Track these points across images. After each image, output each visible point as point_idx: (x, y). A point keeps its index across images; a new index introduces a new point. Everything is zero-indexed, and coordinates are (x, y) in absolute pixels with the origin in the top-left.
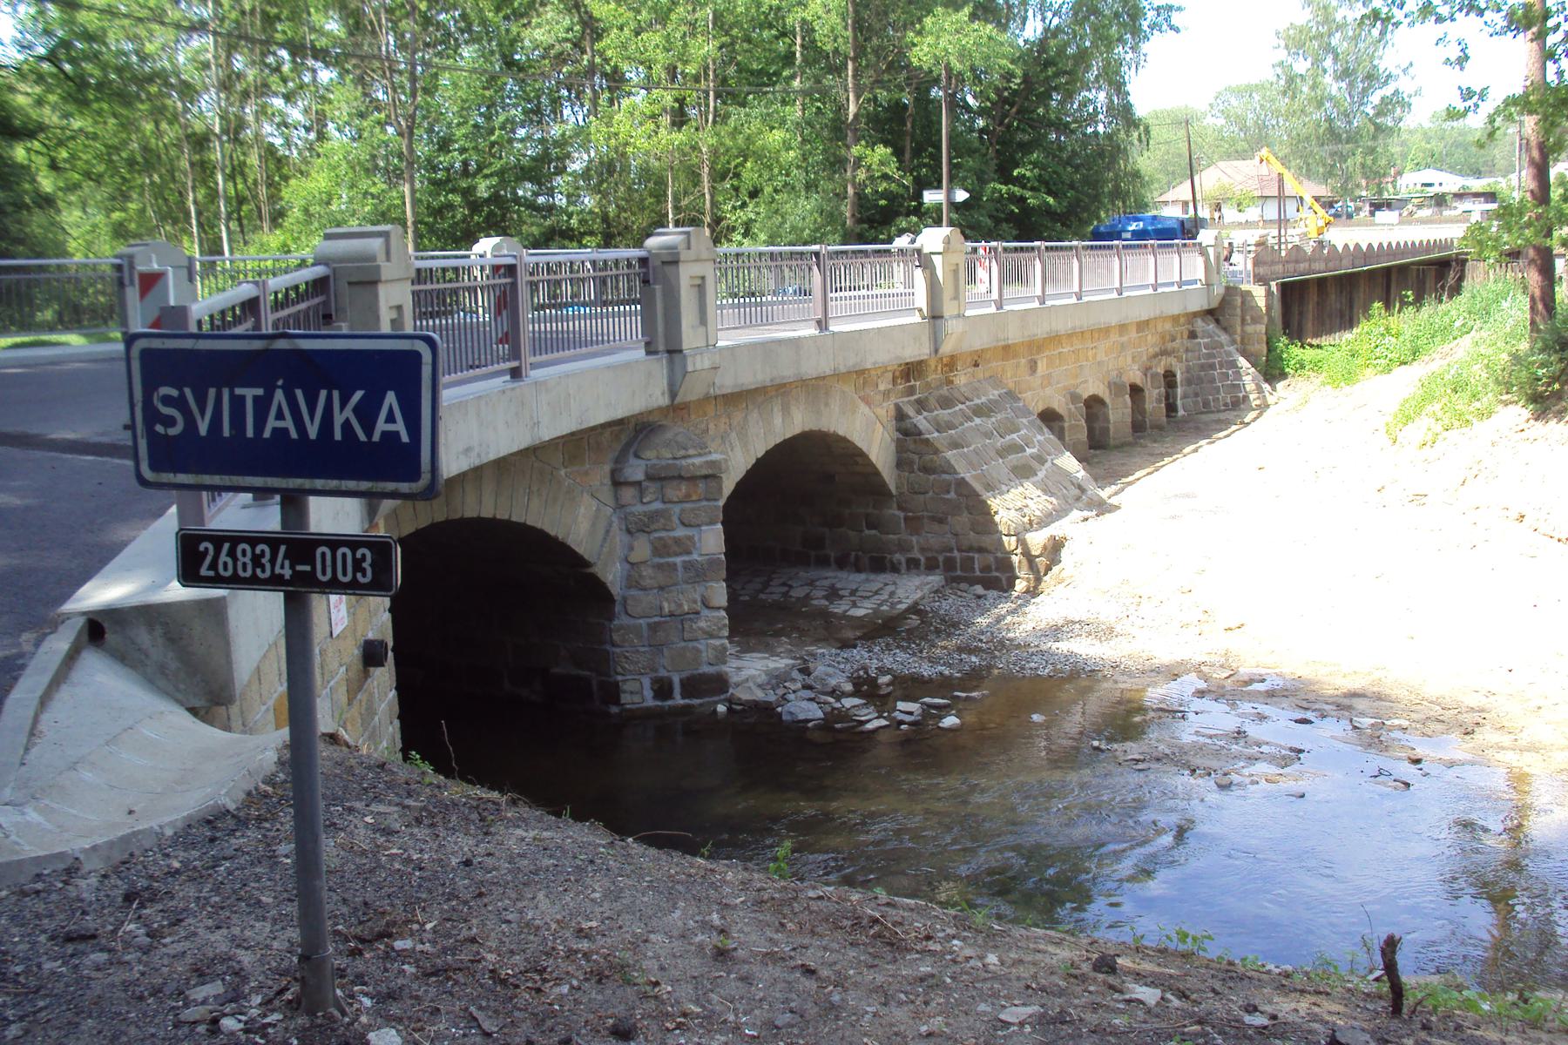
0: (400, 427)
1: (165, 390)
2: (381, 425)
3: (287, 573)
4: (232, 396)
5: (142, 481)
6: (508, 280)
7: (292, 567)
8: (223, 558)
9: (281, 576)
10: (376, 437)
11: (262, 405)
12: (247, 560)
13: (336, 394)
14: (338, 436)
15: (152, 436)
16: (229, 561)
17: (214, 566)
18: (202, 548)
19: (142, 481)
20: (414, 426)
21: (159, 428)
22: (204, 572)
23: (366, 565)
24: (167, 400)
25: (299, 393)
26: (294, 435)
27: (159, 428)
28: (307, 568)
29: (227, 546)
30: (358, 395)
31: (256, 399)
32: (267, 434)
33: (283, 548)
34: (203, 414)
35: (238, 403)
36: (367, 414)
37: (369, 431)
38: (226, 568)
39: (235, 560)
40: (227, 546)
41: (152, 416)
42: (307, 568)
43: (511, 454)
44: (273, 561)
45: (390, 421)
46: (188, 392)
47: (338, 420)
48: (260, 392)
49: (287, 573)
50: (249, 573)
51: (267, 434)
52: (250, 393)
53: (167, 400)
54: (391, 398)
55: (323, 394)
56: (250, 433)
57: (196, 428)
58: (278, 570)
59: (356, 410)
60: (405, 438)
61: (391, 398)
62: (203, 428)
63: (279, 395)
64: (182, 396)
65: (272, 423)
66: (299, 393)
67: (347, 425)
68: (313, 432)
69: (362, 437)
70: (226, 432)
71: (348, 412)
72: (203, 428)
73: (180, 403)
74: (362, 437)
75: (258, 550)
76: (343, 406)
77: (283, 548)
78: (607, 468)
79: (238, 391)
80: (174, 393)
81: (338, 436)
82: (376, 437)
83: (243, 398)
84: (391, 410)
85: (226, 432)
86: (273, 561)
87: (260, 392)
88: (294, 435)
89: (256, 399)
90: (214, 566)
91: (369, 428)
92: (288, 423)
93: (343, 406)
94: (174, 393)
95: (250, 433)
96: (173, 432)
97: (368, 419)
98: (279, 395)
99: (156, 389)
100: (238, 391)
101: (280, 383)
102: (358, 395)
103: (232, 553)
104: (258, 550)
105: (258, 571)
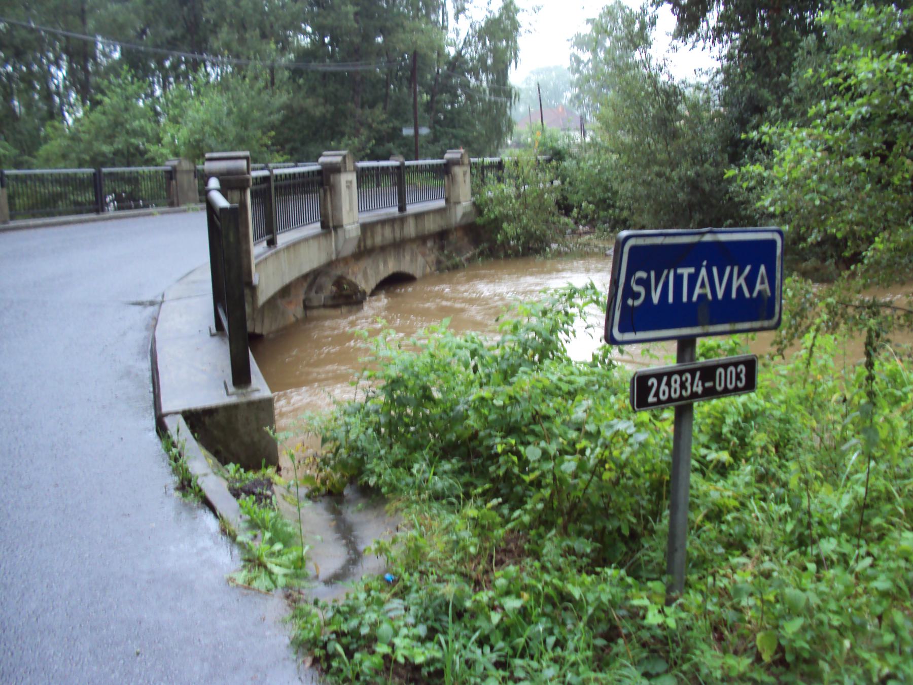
0: (766, 286)
3: (699, 390)
8: (663, 387)
9: (696, 393)
10: (755, 294)
11: (693, 279)
12: (678, 386)
14: (734, 295)
17: (657, 394)
18: (650, 383)
22: (651, 399)
23: (743, 376)
24: (640, 282)
25: (715, 270)
26: (710, 296)
32: (695, 298)
33: (698, 374)
35: (678, 279)
36: (751, 281)
44: (692, 384)
49: (699, 390)
51: (695, 298)
52: (686, 272)
55: (728, 269)
56: (685, 299)
58: (695, 389)
59: (747, 279)
60: (769, 293)
62: (656, 298)
63: (703, 272)
65: (697, 291)
66: (715, 270)
67: (740, 289)
68: (720, 294)
69: (747, 295)
70: (671, 299)
71: (742, 281)
72: (656, 298)
73: (645, 283)
77: (698, 374)
79: (680, 271)
81: (734, 295)
82: (755, 294)
83: (681, 276)
85: (671, 299)
86: (692, 384)
88: (710, 296)
90: (657, 394)
95: (685, 299)
97: (751, 286)
98: (703, 272)
100: (680, 271)
103: (668, 384)
105: (684, 393)
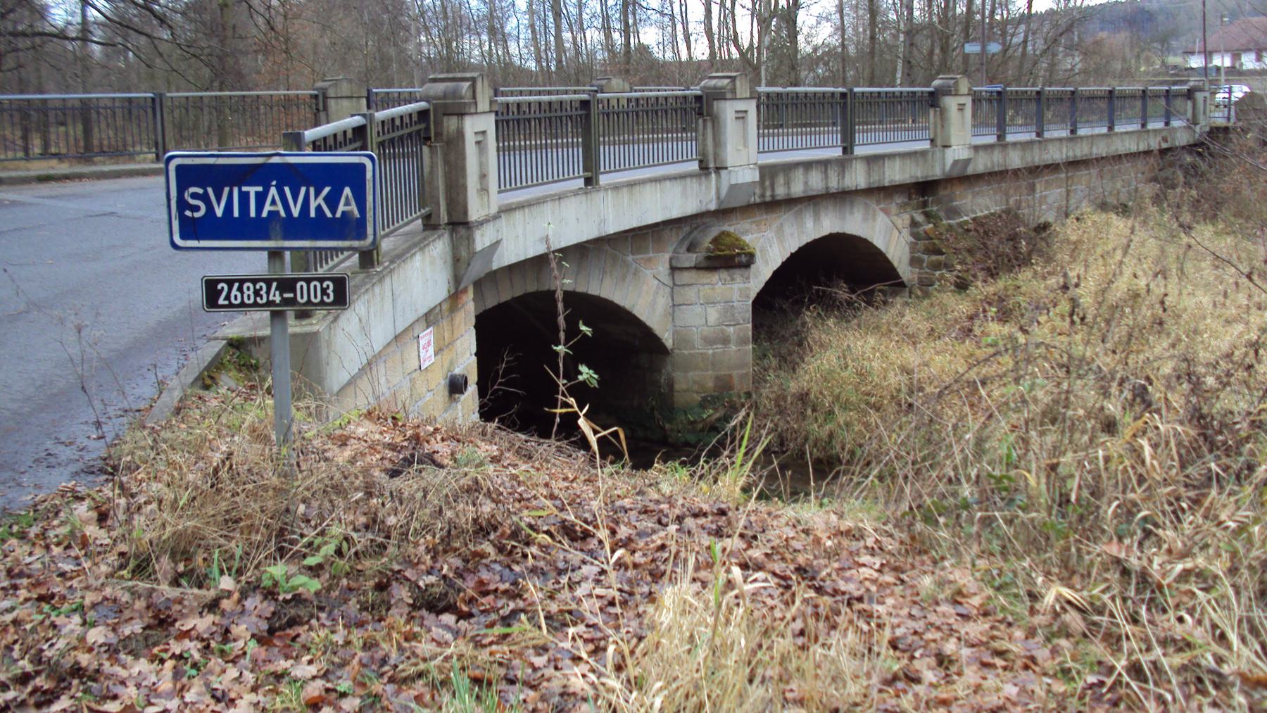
0: (353, 208)
1: (193, 190)
2: (341, 208)
3: (278, 299)
4: (240, 191)
5: (174, 246)
6: (422, 126)
7: (281, 295)
8: (234, 292)
9: (274, 302)
10: (338, 215)
11: (261, 198)
12: (251, 292)
13: (312, 190)
14: (313, 214)
15: (183, 219)
16: (239, 295)
17: (228, 297)
18: (219, 287)
19: (174, 246)
20: (362, 208)
21: (188, 213)
22: (221, 301)
23: (330, 291)
24: (194, 196)
25: (287, 189)
26: (283, 214)
27: (188, 213)
28: (291, 295)
29: (236, 285)
30: (327, 190)
31: (257, 193)
32: (265, 214)
33: (275, 284)
34: (219, 203)
35: (244, 197)
36: (332, 201)
37: (334, 211)
38: (236, 297)
39: (242, 293)
40: (236, 285)
41: (182, 205)
42: (291, 295)
43: (587, 242)
44: (268, 293)
45: (347, 205)
46: (210, 190)
47: (313, 205)
48: (260, 189)
49: (278, 299)
50: (252, 301)
51: (265, 214)
52: (252, 190)
53: (194, 196)
54: (347, 191)
55: (303, 190)
56: (253, 214)
57: (214, 213)
58: (271, 298)
59: (326, 199)
60: (357, 214)
61: (347, 191)
62: (219, 212)
63: (273, 191)
64: (206, 193)
65: (268, 208)
66: (287, 189)
67: (319, 208)
68: (296, 212)
69: (329, 215)
70: (236, 214)
71: (320, 200)
72: (219, 212)
73: (205, 198)
74: (329, 215)
75: (325, 285)
76: (317, 196)
77: (275, 284)
78: (667, 256)
79: (245, 189)
80: (200, 191)
81: (313, 214)
82: (338, 215)
83: (248, 193)
84: (347, 197)
85: (236, 214)
86: (268, 293)
87: (260, 189)
88: (283, 214)
89: (257, 193)
90: (228, 297)
91: (333, 209)
92: (280, 208)
93: (317, 196)
94: (200, 191)
95: (253, 214)
96: (197, 215)
97: (333, 206)
98: (273, 191)
99: (187, 188)
100: (245, 189)
101: (274, 183)
102: (327, 190)
103: (240, 289)
104: (325, 285)
105: (258, 299)
